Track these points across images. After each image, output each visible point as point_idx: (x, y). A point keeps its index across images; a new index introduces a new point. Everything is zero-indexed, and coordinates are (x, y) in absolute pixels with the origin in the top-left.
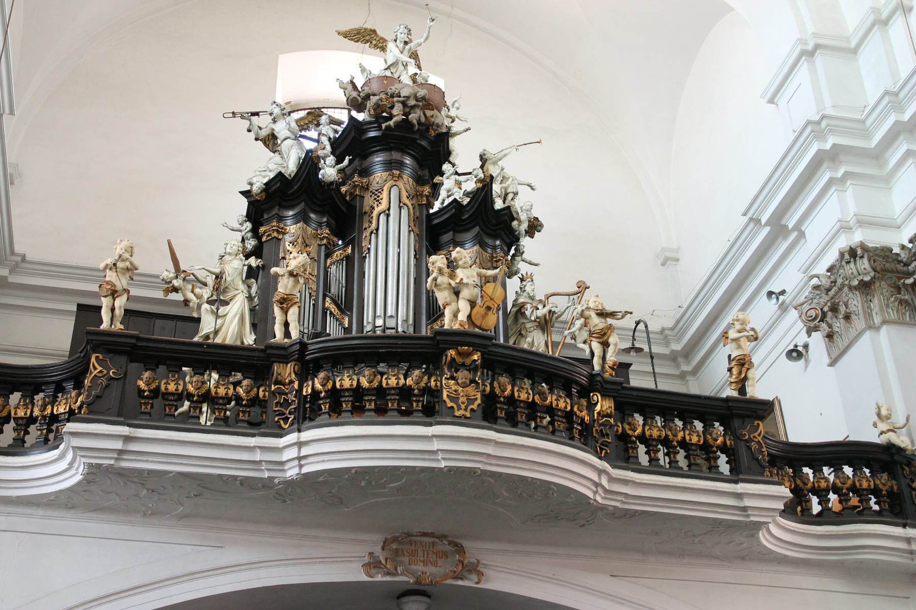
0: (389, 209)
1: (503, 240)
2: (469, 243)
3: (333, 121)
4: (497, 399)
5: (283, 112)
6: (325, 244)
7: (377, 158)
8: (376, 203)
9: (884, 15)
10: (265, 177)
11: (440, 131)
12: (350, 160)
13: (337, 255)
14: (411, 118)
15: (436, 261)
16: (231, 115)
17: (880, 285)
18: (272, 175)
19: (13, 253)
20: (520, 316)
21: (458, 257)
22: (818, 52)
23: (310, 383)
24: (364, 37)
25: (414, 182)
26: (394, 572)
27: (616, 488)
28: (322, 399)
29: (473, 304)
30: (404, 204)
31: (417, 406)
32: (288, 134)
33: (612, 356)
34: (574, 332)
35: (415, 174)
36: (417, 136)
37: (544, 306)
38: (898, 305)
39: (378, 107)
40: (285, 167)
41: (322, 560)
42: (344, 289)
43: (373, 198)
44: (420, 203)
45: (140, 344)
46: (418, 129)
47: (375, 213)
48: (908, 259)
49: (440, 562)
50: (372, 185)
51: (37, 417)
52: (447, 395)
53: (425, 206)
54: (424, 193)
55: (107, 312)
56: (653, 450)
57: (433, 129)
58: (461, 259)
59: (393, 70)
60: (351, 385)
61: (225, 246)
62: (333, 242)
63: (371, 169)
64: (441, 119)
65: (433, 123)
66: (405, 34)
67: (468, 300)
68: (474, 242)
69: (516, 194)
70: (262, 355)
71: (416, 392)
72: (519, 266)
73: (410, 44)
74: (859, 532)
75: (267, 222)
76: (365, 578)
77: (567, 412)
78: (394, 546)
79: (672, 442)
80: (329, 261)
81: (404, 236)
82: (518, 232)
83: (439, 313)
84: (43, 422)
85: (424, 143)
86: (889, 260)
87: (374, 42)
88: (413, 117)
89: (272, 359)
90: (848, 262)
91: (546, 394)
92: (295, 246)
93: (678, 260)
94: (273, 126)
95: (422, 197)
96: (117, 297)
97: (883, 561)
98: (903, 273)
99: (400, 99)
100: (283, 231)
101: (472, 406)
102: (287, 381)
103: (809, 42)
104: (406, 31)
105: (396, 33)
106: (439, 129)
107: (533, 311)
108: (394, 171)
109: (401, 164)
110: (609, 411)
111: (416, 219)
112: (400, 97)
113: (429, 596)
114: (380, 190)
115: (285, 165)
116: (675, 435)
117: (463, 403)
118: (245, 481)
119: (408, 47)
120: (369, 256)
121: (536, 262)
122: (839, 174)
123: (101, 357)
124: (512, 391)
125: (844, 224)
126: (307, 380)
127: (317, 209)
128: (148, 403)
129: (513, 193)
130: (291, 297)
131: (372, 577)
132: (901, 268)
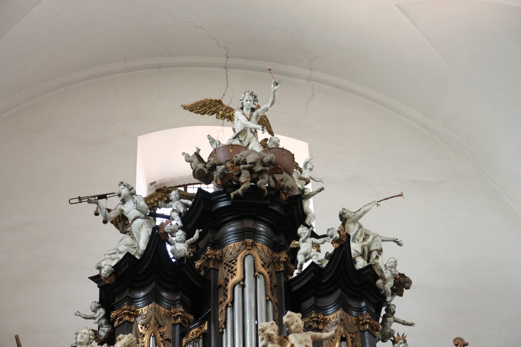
0: (244, 280)
1: (368, 302)
2: (332, 307)
3: (183, 195)
5: (131, 192)
6: (179, 323)
7: (229, 228)
8: (230, 274)
10: (113, 260)
11: (292, 194)
12: (200, 233)
13: (193, 333)
14: (259, 184)
15: (266, 328)
16: (77, 200)
18: (121, 256)
21: (289, 322)
24: (210, 108)
25: (269, 250)
30: (260, 273)
32: (137, 213)
36: (268, 202)
39: (224, 175)
40: (136, 247)
43: (227, 270)
44: (277, 270)
46: (268, 194)
47: (230, 285)
50: (226, 256)
53: (282, 273)
54: (281, 260)
57: (284, 193)
58: (293, 324)
59: (242, 138)
61: (76, 336)
62: (189, 320)
65: (283, 186)
66: (251, 101)
68: (337, 305)
69: (380, 251)
72: (392, 328)
75: (118, 306)
80: (184, 341)
81: (261, 307)
82: (383, 291)
85: (276, 208)
87: (220, 113)
92: (148, 328)
94: (122, 207)
95: (279, 264)
99: (247, 166)
100: (135, 314)
104: (251, 98)
105: (242, 101)
106: (290, 192)
108: (247, 240)
109: (254, 232)
111: (273, 288)
112: (246, 163)
114: (234, 261)
115: (137, 246)
119: (255, 114)
120: (226, 331)
121: (410, 322)
129: (377, 250)
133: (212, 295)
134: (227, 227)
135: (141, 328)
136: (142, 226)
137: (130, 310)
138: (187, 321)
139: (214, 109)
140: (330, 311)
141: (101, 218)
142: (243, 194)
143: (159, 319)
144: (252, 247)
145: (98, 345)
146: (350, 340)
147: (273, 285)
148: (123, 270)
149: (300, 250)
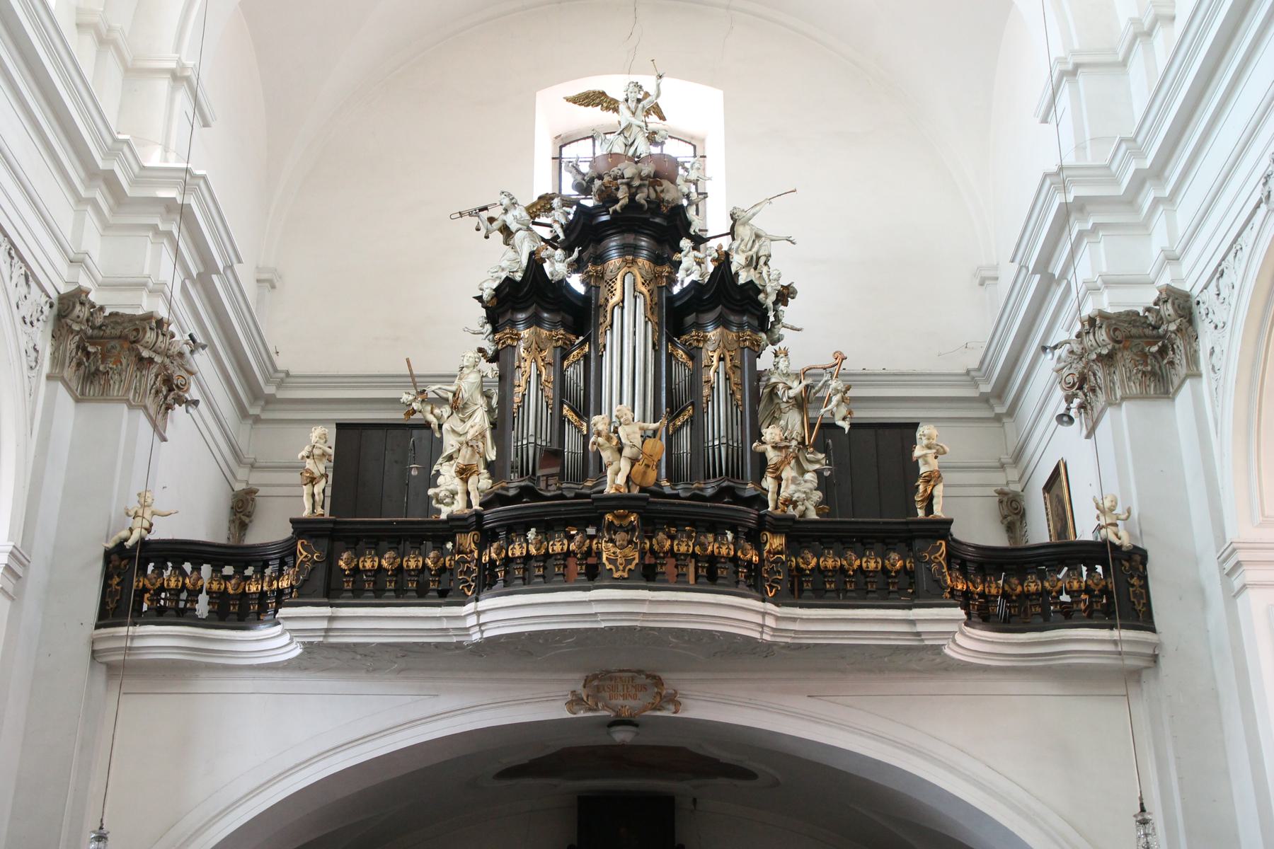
0: (623, 301)
1: (752, 315)
6: (560, 346)
9: (1146, 27)
10: (495, 280)
12: (579, 252)
15: (597, 423)
16: (458, 215)
17: (1123, 356)
19: (276, 370)
20: (774, 397)
22: (1079, 71)
26: (595, 707)
28: (497, 567)
29: (633, 461)
30: (640, 293)
32: (520, 226)
34: (832, 410)
35: (653, 255)
36: (648, 216)
37: (800, 382)
38: (1142, 377)
41: (526, 701)
42: (582, 392)
43: (607, 289)
44: (660, 285)
45: (338, 527)
46: (648, 208)
48: (1156, 322)
49: (640, 695)
51: (267, 591)
52: (607, 558)
55: (308, 500)
56: (828, 581)
57: (664, 206)
58: (622, 417)
60: (522, 553)
62: (570, 341)
64: (670, 194)
71: (579, 556)
73: (642, 103)
74: (1061, 638)
76: (568, 715)
78: (595, 683)
79: (848, 571)
80: (566, 363)
84: (272, 595)
85: (657, 220)
86: (1138, 324)
87: (605, 105)
88: (640, 197)
89: (455, 530)
93: (997, 279)
94: (504, 217)
96: (316, 484)
97: (1090, 664)
98: (1153, 337)
101: (629, 567)
102: (468, 550)
103: (1069, 60)
104: (637, 89)
107: (784, 392)
108: (627, 257)
110: (780, 549)
111: (653, 306)
112: (623, 178)
113: (636, 725)
114: (614, 280)
115: (519, 260)
116: (851, 565)
117: (621, 564)
118: (438, 645)
119: (640, 106)
121: (798, 327)
122: (1089, 226)
123: (306, 543)
124: (672, 546)
125: (1091, 285)
126: (486, 548)
127: (551, 307)
128: (349, 581)
129: (765, 256)
131: (575, 714)
132: (1150, 332)
135: (524, 352)
136: (524, 239)
138: (568, 343)
139: (598, 101)
140: (710, 328)
141: (483, 231)
143: (541, 343)
146: (728, 359)
147: (654, 303)
148: (505, 292)
149: (682, 265)
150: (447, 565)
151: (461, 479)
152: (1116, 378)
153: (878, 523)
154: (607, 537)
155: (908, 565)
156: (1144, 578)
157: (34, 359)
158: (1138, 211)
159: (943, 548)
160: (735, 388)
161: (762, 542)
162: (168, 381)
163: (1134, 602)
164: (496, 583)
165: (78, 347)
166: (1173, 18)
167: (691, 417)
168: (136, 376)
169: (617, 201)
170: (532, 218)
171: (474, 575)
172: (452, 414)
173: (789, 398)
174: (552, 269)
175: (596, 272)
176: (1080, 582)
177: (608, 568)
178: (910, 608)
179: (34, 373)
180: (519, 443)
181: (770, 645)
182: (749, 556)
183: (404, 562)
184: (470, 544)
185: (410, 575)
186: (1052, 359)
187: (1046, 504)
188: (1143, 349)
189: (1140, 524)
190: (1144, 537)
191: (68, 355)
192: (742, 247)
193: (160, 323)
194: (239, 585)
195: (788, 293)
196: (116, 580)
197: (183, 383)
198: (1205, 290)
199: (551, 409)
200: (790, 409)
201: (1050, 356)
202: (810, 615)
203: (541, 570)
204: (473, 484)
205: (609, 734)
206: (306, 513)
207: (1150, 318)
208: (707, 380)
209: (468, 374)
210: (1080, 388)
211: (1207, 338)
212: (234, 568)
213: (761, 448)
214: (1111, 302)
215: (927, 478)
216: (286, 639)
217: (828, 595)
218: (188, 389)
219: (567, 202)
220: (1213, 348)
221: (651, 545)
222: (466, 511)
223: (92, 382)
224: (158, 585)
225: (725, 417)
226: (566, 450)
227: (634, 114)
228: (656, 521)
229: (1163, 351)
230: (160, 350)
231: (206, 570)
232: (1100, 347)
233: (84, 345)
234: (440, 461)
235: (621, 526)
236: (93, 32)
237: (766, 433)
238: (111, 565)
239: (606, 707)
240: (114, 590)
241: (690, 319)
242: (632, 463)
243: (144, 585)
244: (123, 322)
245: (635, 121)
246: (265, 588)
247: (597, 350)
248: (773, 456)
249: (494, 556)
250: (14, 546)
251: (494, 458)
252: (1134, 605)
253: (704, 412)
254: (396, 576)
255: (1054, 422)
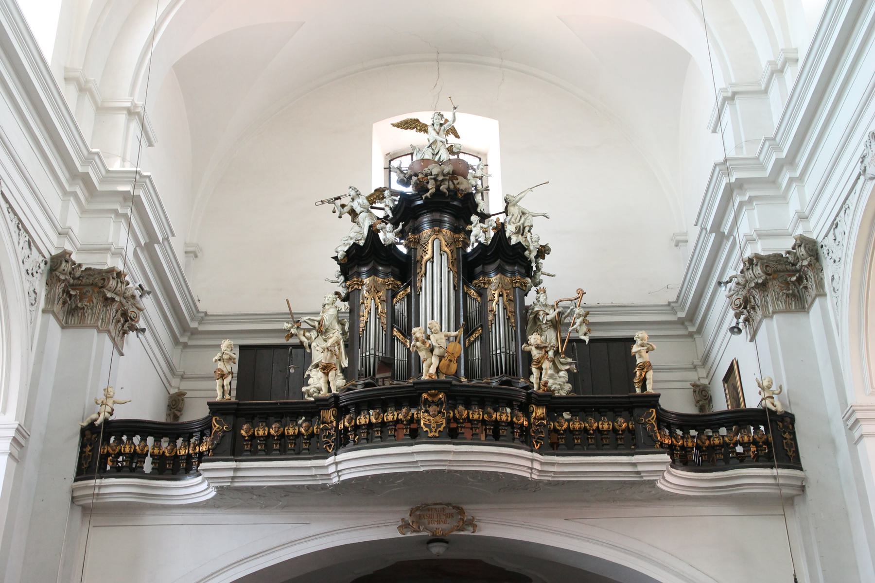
0: (433, 257)
1: (520, 265)
4: (458, 421)
6: (391, 289)
9: (779, 66)
10: (346, 246)
12: (403, 225)
15: (416, 332)
16: (321, 203)
19: (198, 311)
20: (537, 320)
22: (736, 97)
23: (342, 421)
24: (411, 125)
26: (418, 530)
27: (546, 468)
28: (349, 432)
29: (441, 358)
31: (406, 431)
32: (362, 209)
33: (544, 377)
34: (576, 328)
35: (452, 226)
37: (555, 310)
41: (371, 526)
42: (406, 319)
45: (240, 407)
47: (423, 263)
48: (794, 261)
49: (449, 520)
51: (192, 454)
52: (424, 423)
55: (219, 389)
56: (576, 438)
57: (459, 193)
60: (365, 422)
62: (398, 285)
63: (422, 226)
64: (463, 185)
65: (459, 189)
66: (439, 119)
67: (438, 356)
70: (315, 405)
71: (405, 423)
73: (444, 126)
74: (737, 475)
77: (508, 422)
78: (418, 513)
80: (395, 300)
83: (474, 328)
85: (455, 203)
86: (782, 262)
87: (419, 128)
88: (443, 188)
89: (321, 408)
90: (748, 269)
91: (491, 413)
94: (352, 204)
95: (459, 242)
98: (793, 271)
99: (432, 177)
101: (440, 429)
102: (329, 421)
103: (728, 90)
104: (440, 117)
107: (544, 316)
110: (542, 416)
112: (432, 175)
113: (447, 542)
114: (427, 243)
116: (591, 426)
117: (434, 428)
118: (309, 487)
119: (442, 128)
121: (553, 274)
122: (746, 198)
123: (218, 419)
124: (468, 414)
125: (749, 237)
126: (341, 420)
128: (248, 444)
129: (529, 226)
130: (329, 365)
131: (404, 534)
133: (412, 268)
134: (422, 218)
136: (365, 217)
137: (358, 281)
139: (414, 125)
140: (492, 275)
141: (338, 213)
142: (431, 196)
144: (439, 232)
145: (341, 301)
146: (505, 295)
148: (352, 254)
150: (315, 432)
151: (324, 373)
152: (769, 299)
153: (609, 398)
154: (424, 409)
155: (630, 426)
156: (793, 433)
157: (33, 299)
158: (779, 187)
159: (654, 413)
160: (510, 315)
161: (530, 411)
162: (125, 314)
163: (786, 450)
164: (348, 442)
165: (64, 291)
166: (797, 60)
167: (481, 335)
168: (103, 311)
169: (427, 190)
170: (370, 204)
171: (333, 438)
172: (318, 336)
173: (547, 321)
174: (384, 237)
175: (415, 239)
176: (749, 437)
177: (425, 430)
178: (632, 455)
179: (33, 308)
180: (364, 355)
181: (537, 482)
182: (521, 421)
183: (285, 430)
184: (330, 417)
185: (290, 440)
186: (725, 290)
187: (725, 390)
188: (786, 279)
189: (788, 397)
190: (792, 406)
191: (57, 296)
192: (513, 220)
193: (119, 274)
194: (173, 450)
195: (545, 251)
196: (89, 448)
197: (135, 316)
198: (826, 238)
199: (385, 331)
200: (548, 329)
201: (724, 288)
202: (564, 461)
203: (379, 433)
204: (332, 376)
205: (428, 549)
206: (218, 399)
207: (790, 258)
208: (491, 309)
209: (328, 309)
210: (745, 308)
211: (829, 269)
212: (169, 438)
213: (528, 348)
214: (763, 248)
215: (641, 367)
216: (205, 486)
217: (576, 447)
218: (138, 321)
219: (394, 193)
220: (833, 276)
221: (454, 414)
222: (328, 395)
223: (73, 315)
224: (117, 450)
225: (504, 335)
226: (396, 359)
227: (438, 133)
228: (457, 398)
229: (800, 280)
230: (119, 293)
231: (150, 440)
232: (757, 278)
233: (68, 290)
234: (310, 368)
235: (433, 402)
236: (75, 83)
237: (531, 338)
238: (85, 438)
239: (426, 529)
240: (87, 455)
241: (479, 269)
242: (440, 359)
243: (108, 451)
244: (94, 274)
245: (439, 138)
246: (191, 452)
247: (416, 291)
248: (536, 354)
249: (347, 424)
250: (19, 424)
251: (347, 365)
252: (787, 452)
253: (489, 331)
254: (280, 440)
255: (729, 334)
